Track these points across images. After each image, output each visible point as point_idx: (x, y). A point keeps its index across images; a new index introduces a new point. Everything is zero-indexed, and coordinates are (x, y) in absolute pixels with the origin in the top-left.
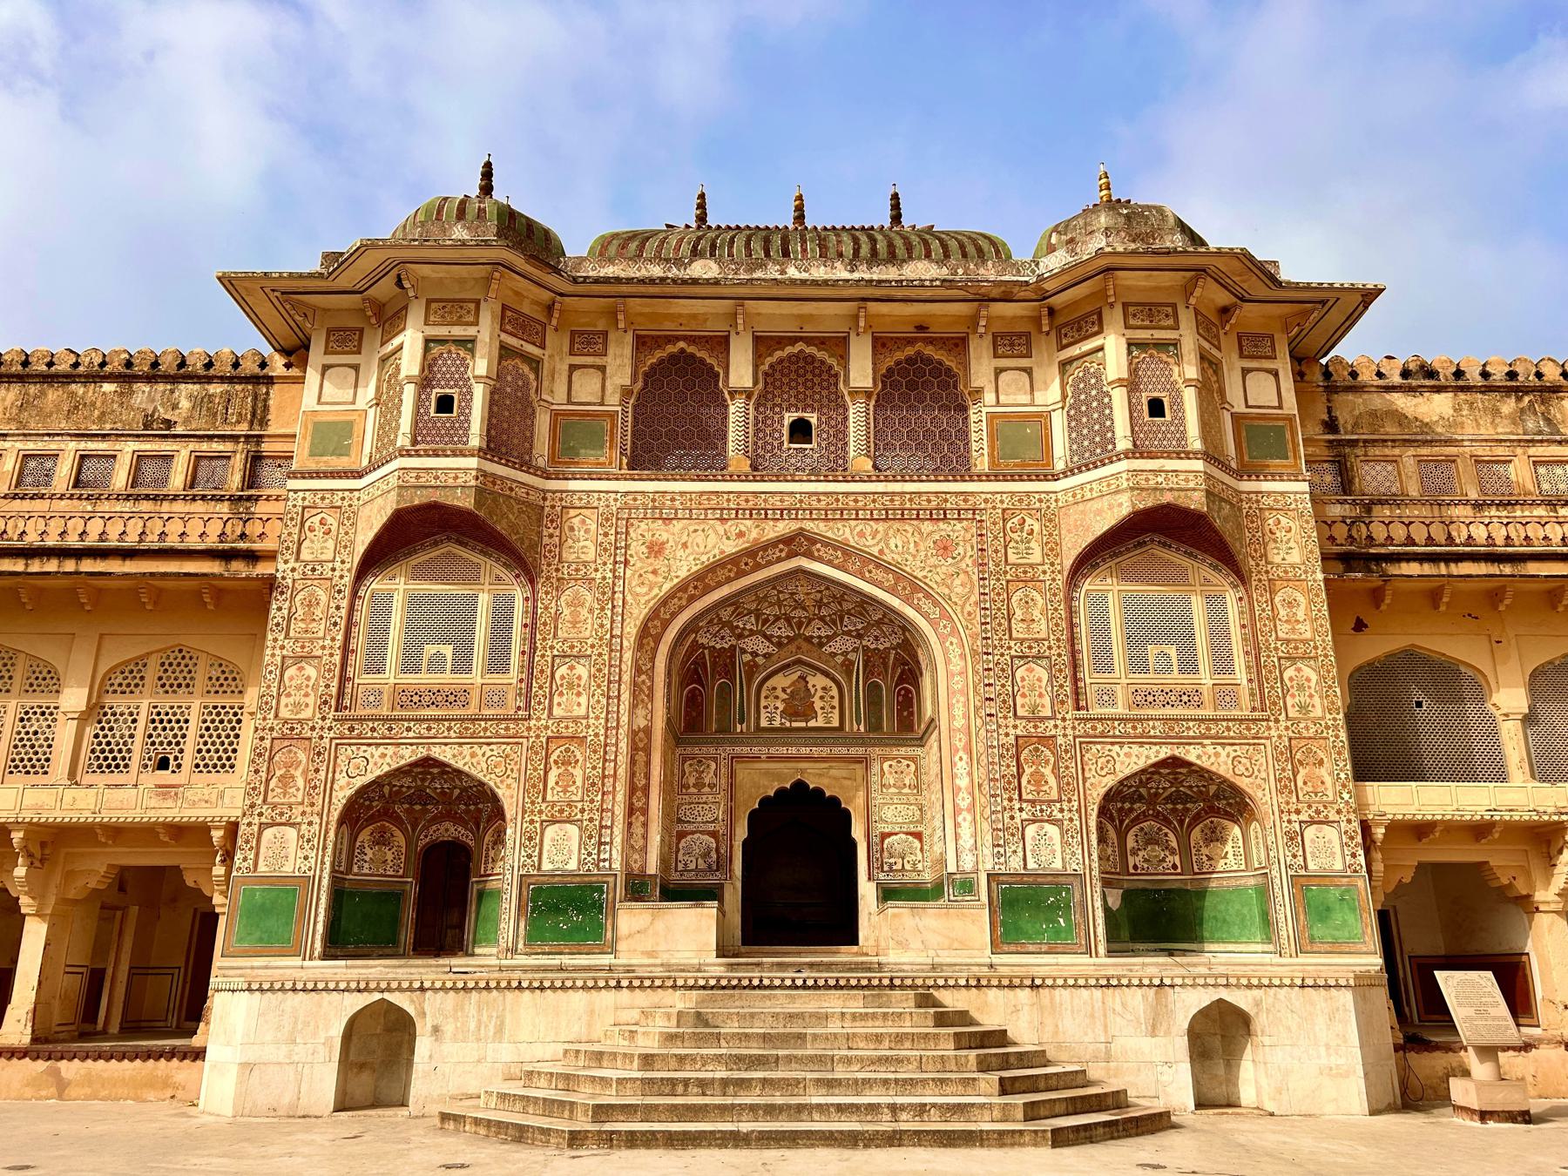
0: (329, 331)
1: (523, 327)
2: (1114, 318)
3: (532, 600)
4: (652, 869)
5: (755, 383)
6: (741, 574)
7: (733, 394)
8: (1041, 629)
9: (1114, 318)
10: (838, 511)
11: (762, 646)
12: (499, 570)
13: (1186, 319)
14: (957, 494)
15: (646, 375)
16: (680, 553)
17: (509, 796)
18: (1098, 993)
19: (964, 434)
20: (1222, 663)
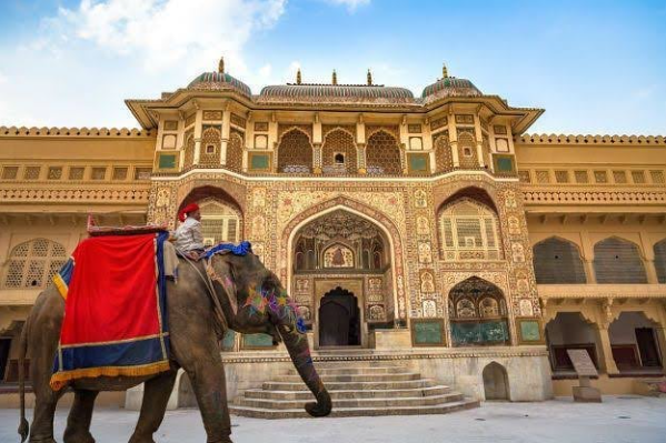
2: (452, 120)
3: (242, 221)
6: (318, 211)
7: (315, 145)
9: (452, 120)
10: (353, 187)
12: (230, 210)
16: (296, 203)
19: (398, 161)
20: (491, 243)
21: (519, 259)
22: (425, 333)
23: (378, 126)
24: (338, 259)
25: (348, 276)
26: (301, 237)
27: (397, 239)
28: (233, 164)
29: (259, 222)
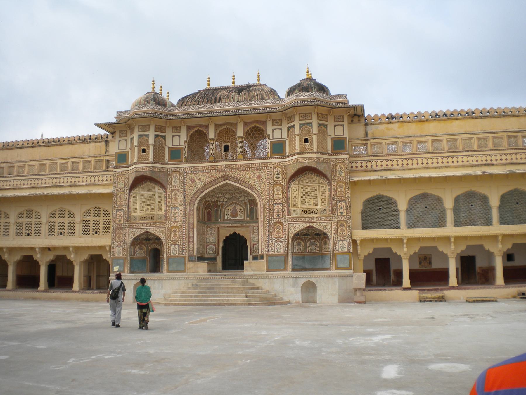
0: (120, 131)
1: (160, 129)
2: (297, 118)
4: (195, 254)
5: (215, 136)
7: (210, 140)
8: (281, 196)
9: (297, 118)
11: (225, 200)
12: (160, 188)
13: (315, 117)
14: (262, 163)
15: (190, 136)
17: (163, 239)
18: (283, 279)
20: (323, 202)
21: (342, 213)
22: (274, 263)
23: (252, 123)
24: (234, 214)
25: (240, 225)
26: (206, 201)
27: (262, 202)
28: (158, 158)
29: (175, 194)
